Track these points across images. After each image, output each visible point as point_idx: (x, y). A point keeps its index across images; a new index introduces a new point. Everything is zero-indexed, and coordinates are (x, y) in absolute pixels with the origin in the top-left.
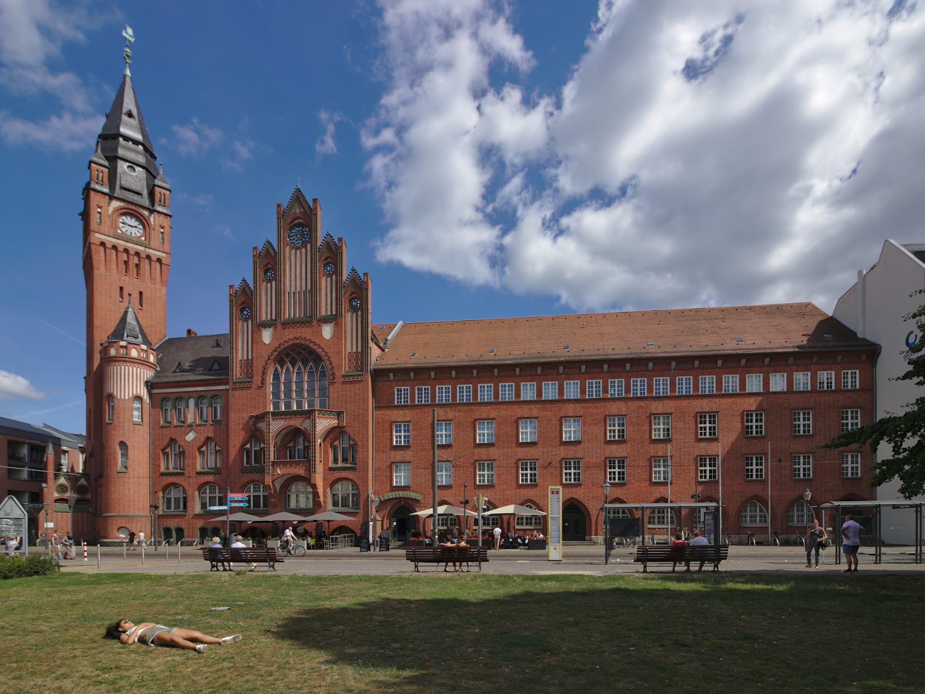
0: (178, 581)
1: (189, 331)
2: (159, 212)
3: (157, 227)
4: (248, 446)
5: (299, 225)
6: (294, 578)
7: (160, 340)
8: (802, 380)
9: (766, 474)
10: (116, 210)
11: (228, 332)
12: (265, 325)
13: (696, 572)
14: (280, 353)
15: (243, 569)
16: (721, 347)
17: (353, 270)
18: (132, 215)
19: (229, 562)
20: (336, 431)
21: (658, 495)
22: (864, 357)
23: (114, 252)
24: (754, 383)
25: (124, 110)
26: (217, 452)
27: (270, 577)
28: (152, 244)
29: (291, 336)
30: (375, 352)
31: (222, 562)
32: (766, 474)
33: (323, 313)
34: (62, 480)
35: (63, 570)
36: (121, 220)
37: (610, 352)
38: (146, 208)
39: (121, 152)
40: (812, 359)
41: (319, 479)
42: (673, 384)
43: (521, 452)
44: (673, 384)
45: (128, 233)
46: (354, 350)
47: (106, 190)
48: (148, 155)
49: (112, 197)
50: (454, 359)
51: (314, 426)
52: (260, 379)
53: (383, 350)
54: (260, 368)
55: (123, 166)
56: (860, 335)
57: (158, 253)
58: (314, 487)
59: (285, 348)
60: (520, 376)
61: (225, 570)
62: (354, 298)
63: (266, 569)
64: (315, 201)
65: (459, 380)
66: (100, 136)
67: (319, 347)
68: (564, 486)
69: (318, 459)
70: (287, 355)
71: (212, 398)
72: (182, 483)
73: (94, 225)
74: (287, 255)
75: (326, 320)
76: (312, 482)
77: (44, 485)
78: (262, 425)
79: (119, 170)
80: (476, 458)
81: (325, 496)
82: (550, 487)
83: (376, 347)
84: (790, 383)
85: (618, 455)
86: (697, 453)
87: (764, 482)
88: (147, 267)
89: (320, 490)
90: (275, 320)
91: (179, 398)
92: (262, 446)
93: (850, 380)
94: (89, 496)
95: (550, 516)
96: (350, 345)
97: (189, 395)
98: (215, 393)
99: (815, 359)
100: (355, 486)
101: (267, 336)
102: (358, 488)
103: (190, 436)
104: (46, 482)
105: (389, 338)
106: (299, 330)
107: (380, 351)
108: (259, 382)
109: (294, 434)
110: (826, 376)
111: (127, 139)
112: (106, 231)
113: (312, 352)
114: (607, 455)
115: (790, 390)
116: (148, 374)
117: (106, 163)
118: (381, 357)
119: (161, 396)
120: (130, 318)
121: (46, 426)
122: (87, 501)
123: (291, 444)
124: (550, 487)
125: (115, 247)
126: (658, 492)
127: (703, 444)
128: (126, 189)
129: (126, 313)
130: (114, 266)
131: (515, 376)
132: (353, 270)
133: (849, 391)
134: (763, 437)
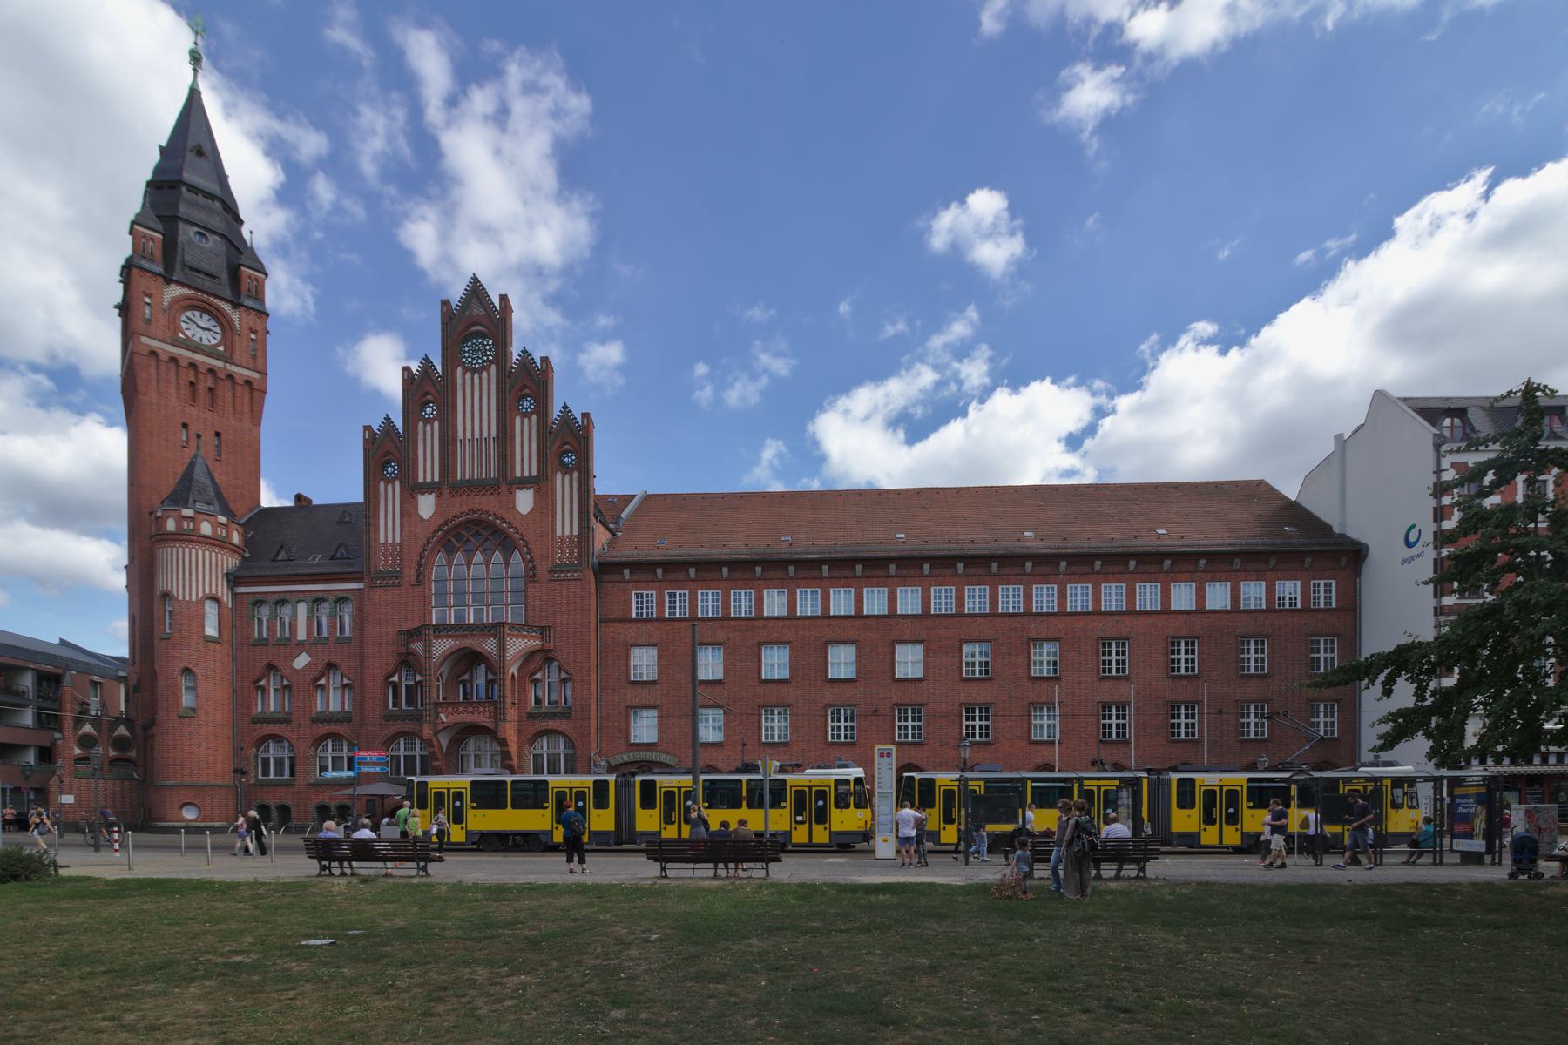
0: (257, 892)
1: (299, 498)
2: (248, 308)
3: (245, 332)
4: (395, 678)
6: (459, 887)
7: (251, 510)
8: (1254, 593)
9: (1201, 731)
10: (175, 301)
11: (361, 499)
12: (427, 488)
13: (1110, 879)
14: (446, 533)
15: (372, 872)
16: (1134, 542)
17: (565, 407)
18: (203, 310)
19: (350, 860)
20: (538, 657)
21: (1040, 761)
22: (1344, 561)
23: (173, 366)
24: (1183, 597)
25: (191, 143)
26: (344, 686)
27: (418, 885)
28: (236, 357)
29: (465, 508)
30: (601, 536)
31: (341, 860)
32: (1201, 731)
33: (518, 474)
34: (88, 728)
35: (63, 872)
36: (184, 318)
37: (968, 545)
38: (226, 301)
39: (183, 210)
40: (1267, 562)
41: (510, 732)
42: (1062, 595)
43: (829, 694)
44: (1062, 595)
45: (197, 339)
46: (567, 532)
47: (159, 270)
48: (229, 217)
49: (169, 281)
50: (726, 551)
51: (502, 648)
52: (413, 572)
53: (614, 534)
54: (415, 557)
55: (187, 233)
56: (1336, 530)
57: (246, 372)
58: (503, 742)
59: (456, 527)
60: (829, 578)
61: (343, 874)
62: (567, 452)
63: (414, 872)
65: (733, 582)
66: (149, 184)
68: (898, 744)
69: (509, 700)
70: (459, 537)
71: (336, 602)
72: (287, 734)
73: (138, 324)
74: (459, 381)
75: (523, 483)
76: (501, 735)
77: (57, 735)
78: (418, 646)
79: (181, 238)
80: (761, 701)
81: (520, 757)
82: (877, 747)
83: (602, 529)
84: (1236, 597)
85: (979, 700)
86: (1098, 699)
87: (1199, 742)
88: (229, 394)
89: (513, 749)
90: (439, 483)
91: (281, 601)
92: (419, 678)
93: (1322, 594)
94: (133, 754)
95: (877, 790)
96: (565, 524)
97: (299, 597)
98: (341, 594)
99: (1272, 563)
100: (570, 743)
101: (426, 506)
102: (573, 747)
103: (301, 661)
104: (60, 731)
105: (623, 515)
106: (478, 499)
107: (609, 535)
108: (413, 578)
109: (469, 659)
110: (1289, 589)
111: (193, 189)
112: (160, 334)
113: (497, 531)
114: (963, 700)
115: (1236, 609)
116: (231, 562)
117: (160, 227)
118: (611, 544)
119: (252, 599)
120: (199, 474)
121: (63, 643)
122: (128, 760)
123: (466, 677)
124: (877, 747)
125: (173, 359)
126: (1041, 755)
127: (1108, 685)
128: (191, 269)
129: (192, 464)
130: (173, 390)
131: (821, 578)
132: (565, 407)
133: (1321, 610)
134: (1196, 677)
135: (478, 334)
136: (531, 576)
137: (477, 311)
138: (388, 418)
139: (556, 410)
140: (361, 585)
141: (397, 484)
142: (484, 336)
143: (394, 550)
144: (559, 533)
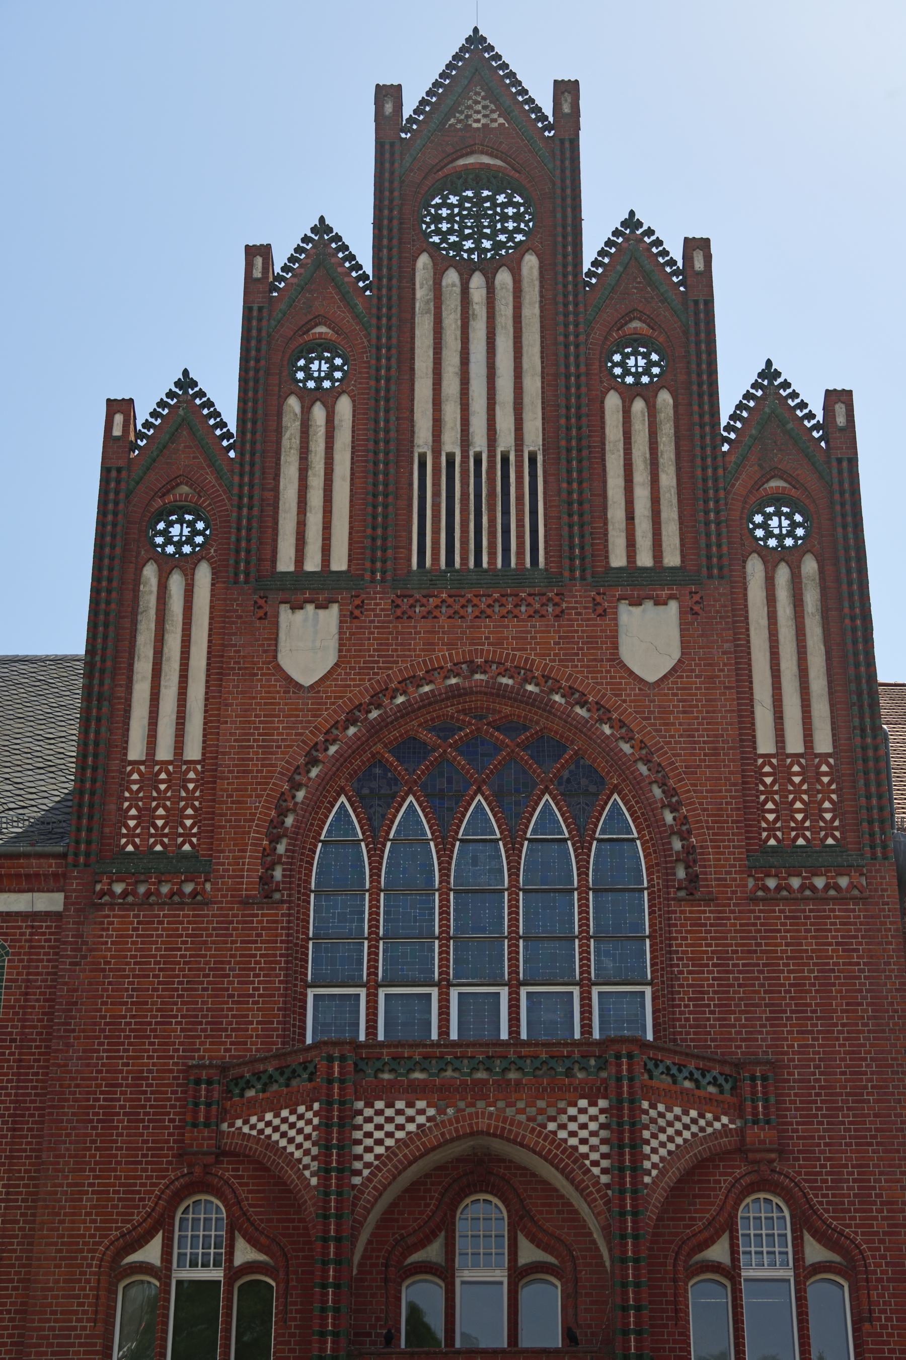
5: (479, 178)
12: (309, 589)
17: (769, 373)
64: (566, 91)
67: (602, 712)
74: (422, 293)
101: (308, 644)
132: (769, 373)
135: (479, 178)
136: (684, 885)
137: (481, 116)
138: (186, 382)
139: (733, 386)
140: (49, 902)
141: (204, 575)
142: (499, 182)
143: (177, 781)
144: (765, 744)
